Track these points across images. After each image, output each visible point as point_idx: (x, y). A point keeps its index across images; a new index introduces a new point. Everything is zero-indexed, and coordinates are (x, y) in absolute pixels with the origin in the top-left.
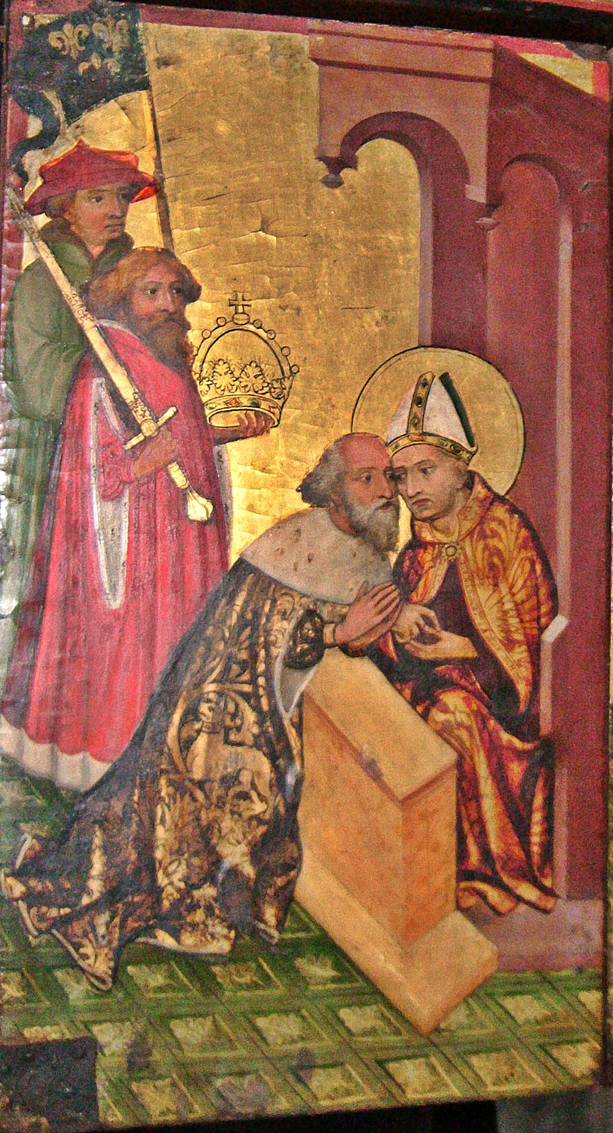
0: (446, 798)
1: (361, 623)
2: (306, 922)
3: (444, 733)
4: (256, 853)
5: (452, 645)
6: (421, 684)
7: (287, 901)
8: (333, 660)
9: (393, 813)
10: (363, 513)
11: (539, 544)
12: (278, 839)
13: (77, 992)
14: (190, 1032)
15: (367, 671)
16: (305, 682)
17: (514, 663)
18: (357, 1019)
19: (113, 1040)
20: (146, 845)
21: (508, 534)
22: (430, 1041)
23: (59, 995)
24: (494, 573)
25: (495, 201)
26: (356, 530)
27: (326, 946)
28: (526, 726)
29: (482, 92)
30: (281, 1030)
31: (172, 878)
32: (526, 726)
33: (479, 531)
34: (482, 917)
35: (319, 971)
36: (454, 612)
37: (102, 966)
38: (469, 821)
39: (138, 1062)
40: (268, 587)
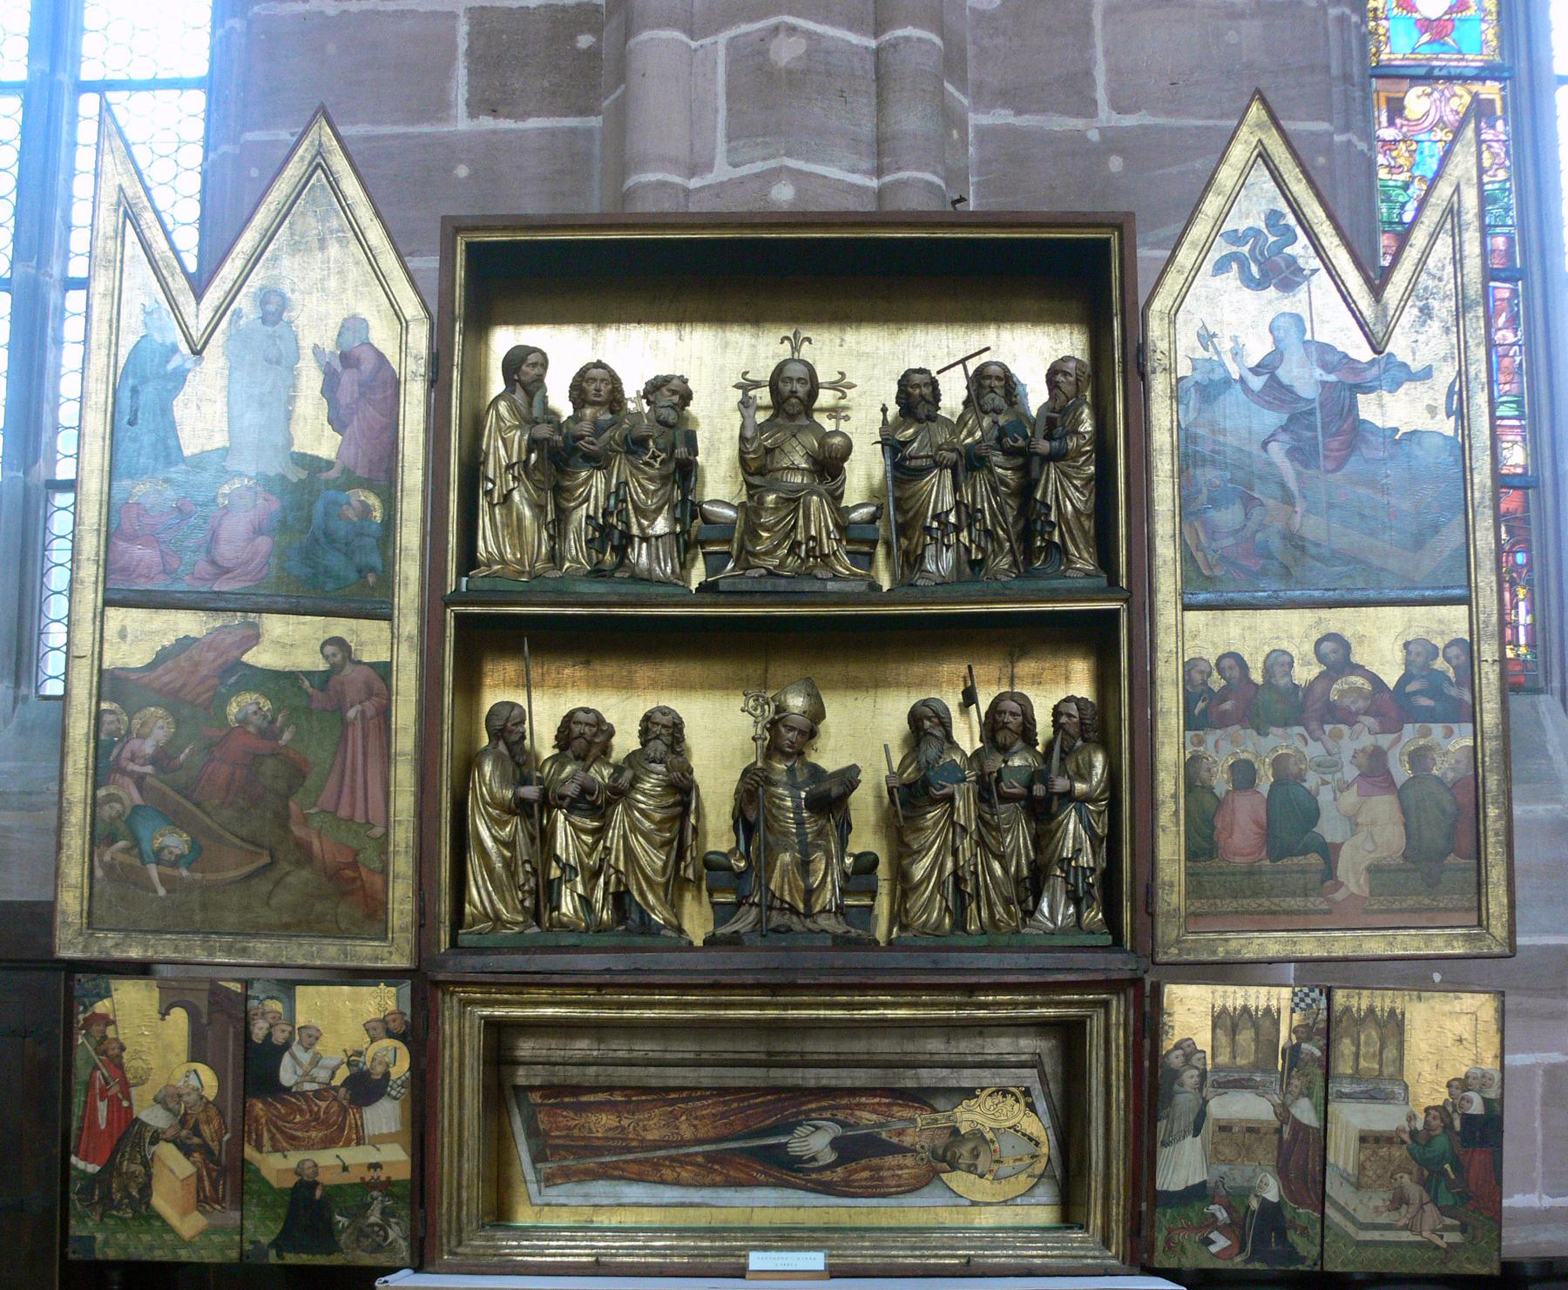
0: (194, 1180)
1: (169, 1134)
2: (153, 1210)
3: (194, 1163)
4: (140, 1191)
5: (196, 1140)
6: (187, 1151)
7: (148, 1205)
8: (162, 1144)
9: (178, 1184)
10: (171, 1105)
11: (221, 1114)
12: (146, 1190)
13: (91, 1224)
14: (121, 1237)
15: (171, 1146)
16: (154, 1148)
17: (214, 1146)
18: (167, 1237)
19: (99, 1237)
20: (110, 1188)
21: (213, 1112)
22: (187, 1244)
23: (85, 1224)
24: (208, 1122)
26: (169, 1110)
27: (159, 1217)
28: (218, 1163)
30: (146, 1238)
31: (118, 1196)
32: (218, 1163)
33: (205, 1110)
34: (203, 1212)
35: (158, 1224)
36: (196, 1131)
37: (97, 1218)
38: (200, 1188)
39: (106, 1242)
40: (144, 1125)
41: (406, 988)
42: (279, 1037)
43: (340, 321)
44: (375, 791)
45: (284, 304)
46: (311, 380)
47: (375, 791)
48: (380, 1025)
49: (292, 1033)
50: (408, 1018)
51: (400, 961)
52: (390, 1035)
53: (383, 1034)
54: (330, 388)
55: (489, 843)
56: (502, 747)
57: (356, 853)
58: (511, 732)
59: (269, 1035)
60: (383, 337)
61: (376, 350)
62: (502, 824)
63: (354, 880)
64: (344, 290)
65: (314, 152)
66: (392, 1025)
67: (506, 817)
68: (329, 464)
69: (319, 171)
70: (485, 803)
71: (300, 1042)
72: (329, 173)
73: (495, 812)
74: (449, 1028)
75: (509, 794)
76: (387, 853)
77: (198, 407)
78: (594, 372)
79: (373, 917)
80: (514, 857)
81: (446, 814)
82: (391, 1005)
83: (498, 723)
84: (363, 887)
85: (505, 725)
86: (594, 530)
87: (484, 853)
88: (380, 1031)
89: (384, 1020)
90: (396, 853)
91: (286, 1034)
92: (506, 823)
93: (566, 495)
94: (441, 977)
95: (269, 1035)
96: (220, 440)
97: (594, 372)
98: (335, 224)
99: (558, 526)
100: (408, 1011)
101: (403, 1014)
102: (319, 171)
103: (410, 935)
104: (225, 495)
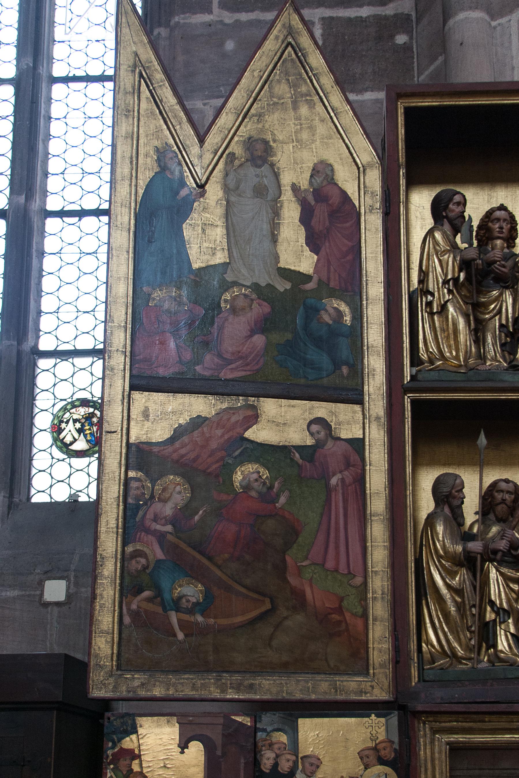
25: (224, 754)
29: (221, 727)
41: (394, 719)
42: (285, 766)
43: (311, 165)
44: (355, 548)
45: (268, 149)
46: (291, 212)
47: (355, 548)
48: (370, 752)
49: (296, 763)
50: (396, 746)
51: (380, 694)
52: (382, 761)
53: (375, 761)
54: (306, 219)
55: (444, 591)
56: (447, 510)
57: (342, 599)
58: (454, 497)
59: (276, 765)
60: (346, 180)
61: (340, 189)
62: (452, 574)
63: (339, 623)
64: (313, 141)
65: (285, 33)
66: (382, 753)
67: (455, 569)
68: (308, 278)
69: (290, 49)
70: (439, 557)
71: (303, 771)
72: (297, 49)
73: (447, 564)
74: (424, 752)
75: (459, 548)
76: (366, 599)
77: (203, 230)
78: (498, 214)
79: (357, 658)
80: (463, 601)
81: (412, 565)
82: (382, 736)
83: (445, 490)
84: (347, 630)
85: (450, 492)
86: (506, 336)
87: (440, 599)
88: (373, 759)
89: (375, 749)
90: (374, 599)
91: (291, 764)
92: (456, 573)
93: (482, 309)
94: (420, 708)
95: (276, 765)
96: (220, 258)
97: (498, 214)
98: (304, 89)
99: (478, 331)
100: (396, 740)
101: (393, 742)
102: (290, 49)
103: (389, 671)
104: (226, 301)
